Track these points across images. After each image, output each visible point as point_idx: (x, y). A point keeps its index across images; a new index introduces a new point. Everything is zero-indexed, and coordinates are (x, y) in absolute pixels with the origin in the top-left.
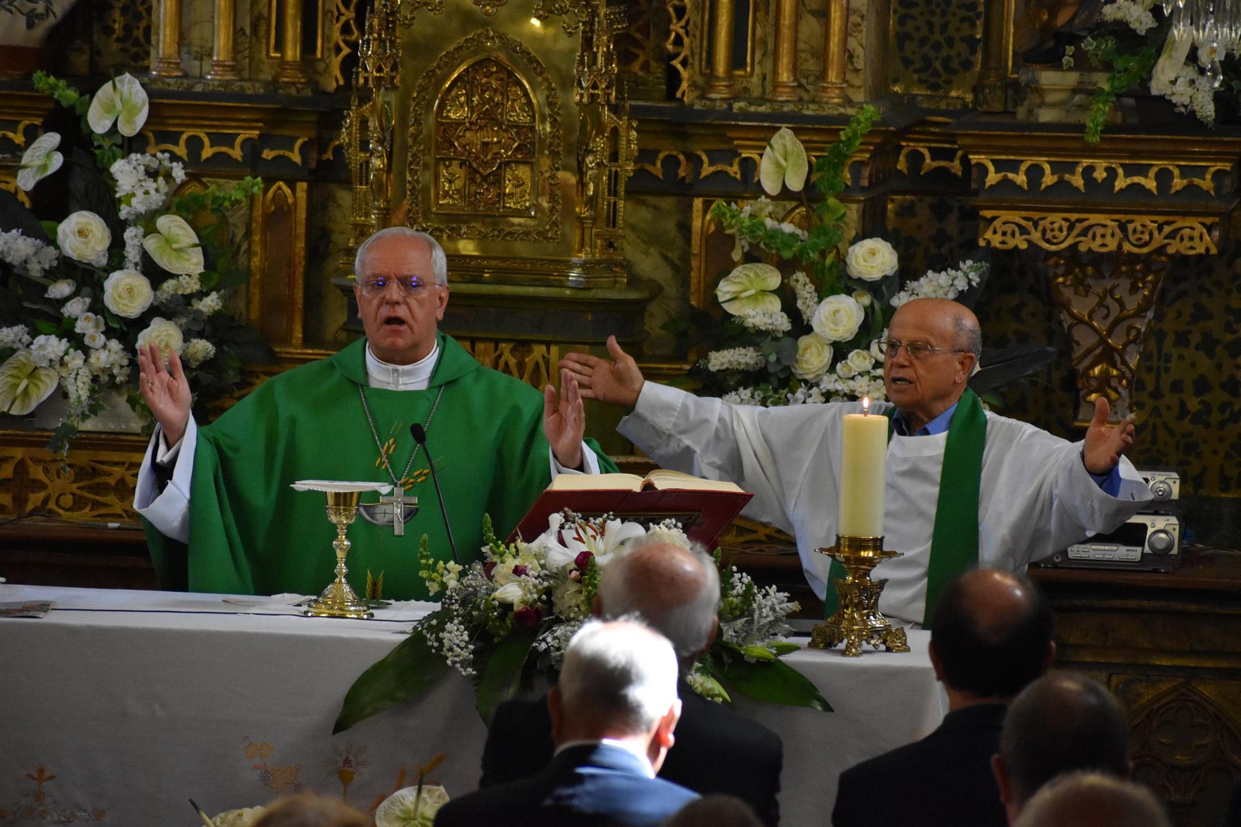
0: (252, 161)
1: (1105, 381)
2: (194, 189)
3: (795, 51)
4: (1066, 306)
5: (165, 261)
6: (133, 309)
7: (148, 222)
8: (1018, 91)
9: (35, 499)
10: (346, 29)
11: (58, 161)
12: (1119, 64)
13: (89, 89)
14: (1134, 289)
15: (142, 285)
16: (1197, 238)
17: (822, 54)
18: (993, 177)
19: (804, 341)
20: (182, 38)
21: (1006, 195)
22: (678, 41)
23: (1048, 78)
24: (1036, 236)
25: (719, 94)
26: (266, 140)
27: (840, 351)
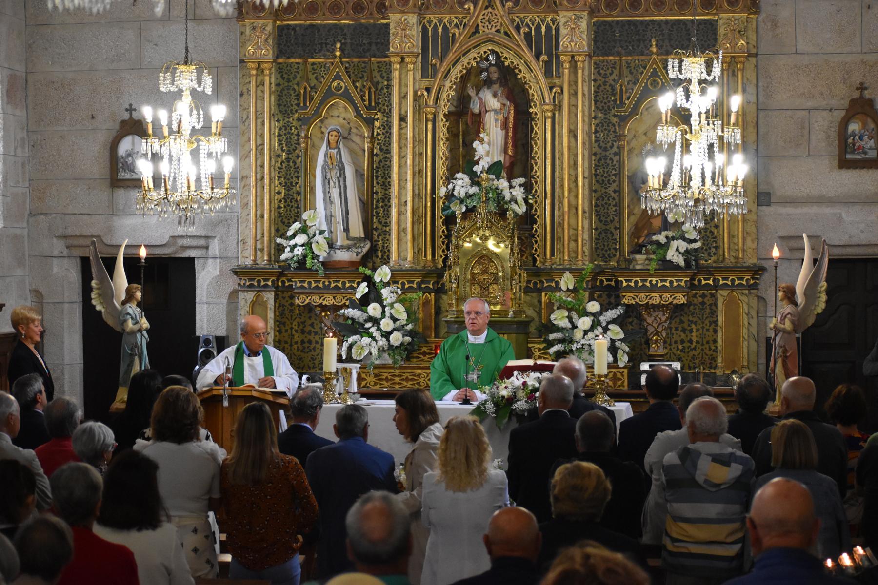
0: (419, 288)
1: (657, 341)
2: (403, 296)
3: (569, 251)
4: (645, 320)
5: (396, 316)
6: (389, 330)
7: (392, 305)
8: (630, 261)
9: (363, 383)
10: (443, 251)
11: (367, 290)
12: (658, 252)
13: (374, 269)
14: (664, 315)
15: (391, 322)
16: (681, 299)
17: (576, 252)
18: (625, 284)
19: (575, 330)
20: (399, 256)
21: (629, 289)
22: (536, 250)
23: (638, 257)
24: (637, 300)
25: (548, 264)
26: (422, 282)
27: (586, 332)
